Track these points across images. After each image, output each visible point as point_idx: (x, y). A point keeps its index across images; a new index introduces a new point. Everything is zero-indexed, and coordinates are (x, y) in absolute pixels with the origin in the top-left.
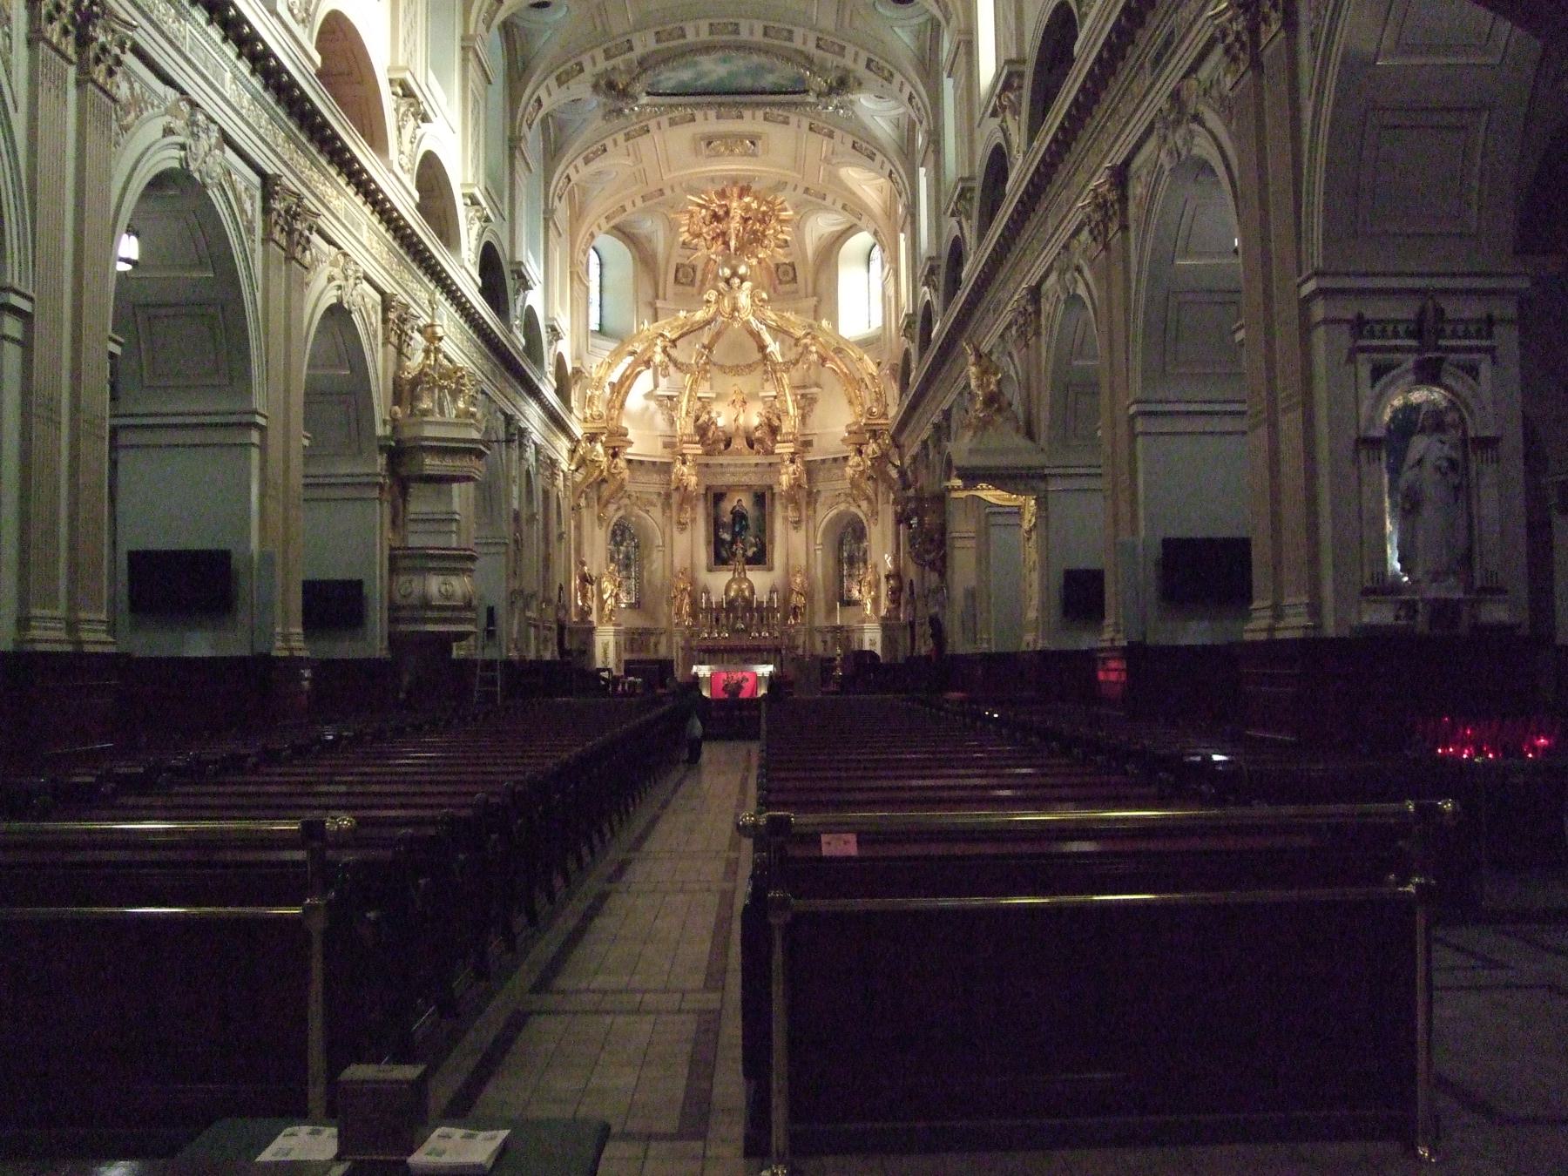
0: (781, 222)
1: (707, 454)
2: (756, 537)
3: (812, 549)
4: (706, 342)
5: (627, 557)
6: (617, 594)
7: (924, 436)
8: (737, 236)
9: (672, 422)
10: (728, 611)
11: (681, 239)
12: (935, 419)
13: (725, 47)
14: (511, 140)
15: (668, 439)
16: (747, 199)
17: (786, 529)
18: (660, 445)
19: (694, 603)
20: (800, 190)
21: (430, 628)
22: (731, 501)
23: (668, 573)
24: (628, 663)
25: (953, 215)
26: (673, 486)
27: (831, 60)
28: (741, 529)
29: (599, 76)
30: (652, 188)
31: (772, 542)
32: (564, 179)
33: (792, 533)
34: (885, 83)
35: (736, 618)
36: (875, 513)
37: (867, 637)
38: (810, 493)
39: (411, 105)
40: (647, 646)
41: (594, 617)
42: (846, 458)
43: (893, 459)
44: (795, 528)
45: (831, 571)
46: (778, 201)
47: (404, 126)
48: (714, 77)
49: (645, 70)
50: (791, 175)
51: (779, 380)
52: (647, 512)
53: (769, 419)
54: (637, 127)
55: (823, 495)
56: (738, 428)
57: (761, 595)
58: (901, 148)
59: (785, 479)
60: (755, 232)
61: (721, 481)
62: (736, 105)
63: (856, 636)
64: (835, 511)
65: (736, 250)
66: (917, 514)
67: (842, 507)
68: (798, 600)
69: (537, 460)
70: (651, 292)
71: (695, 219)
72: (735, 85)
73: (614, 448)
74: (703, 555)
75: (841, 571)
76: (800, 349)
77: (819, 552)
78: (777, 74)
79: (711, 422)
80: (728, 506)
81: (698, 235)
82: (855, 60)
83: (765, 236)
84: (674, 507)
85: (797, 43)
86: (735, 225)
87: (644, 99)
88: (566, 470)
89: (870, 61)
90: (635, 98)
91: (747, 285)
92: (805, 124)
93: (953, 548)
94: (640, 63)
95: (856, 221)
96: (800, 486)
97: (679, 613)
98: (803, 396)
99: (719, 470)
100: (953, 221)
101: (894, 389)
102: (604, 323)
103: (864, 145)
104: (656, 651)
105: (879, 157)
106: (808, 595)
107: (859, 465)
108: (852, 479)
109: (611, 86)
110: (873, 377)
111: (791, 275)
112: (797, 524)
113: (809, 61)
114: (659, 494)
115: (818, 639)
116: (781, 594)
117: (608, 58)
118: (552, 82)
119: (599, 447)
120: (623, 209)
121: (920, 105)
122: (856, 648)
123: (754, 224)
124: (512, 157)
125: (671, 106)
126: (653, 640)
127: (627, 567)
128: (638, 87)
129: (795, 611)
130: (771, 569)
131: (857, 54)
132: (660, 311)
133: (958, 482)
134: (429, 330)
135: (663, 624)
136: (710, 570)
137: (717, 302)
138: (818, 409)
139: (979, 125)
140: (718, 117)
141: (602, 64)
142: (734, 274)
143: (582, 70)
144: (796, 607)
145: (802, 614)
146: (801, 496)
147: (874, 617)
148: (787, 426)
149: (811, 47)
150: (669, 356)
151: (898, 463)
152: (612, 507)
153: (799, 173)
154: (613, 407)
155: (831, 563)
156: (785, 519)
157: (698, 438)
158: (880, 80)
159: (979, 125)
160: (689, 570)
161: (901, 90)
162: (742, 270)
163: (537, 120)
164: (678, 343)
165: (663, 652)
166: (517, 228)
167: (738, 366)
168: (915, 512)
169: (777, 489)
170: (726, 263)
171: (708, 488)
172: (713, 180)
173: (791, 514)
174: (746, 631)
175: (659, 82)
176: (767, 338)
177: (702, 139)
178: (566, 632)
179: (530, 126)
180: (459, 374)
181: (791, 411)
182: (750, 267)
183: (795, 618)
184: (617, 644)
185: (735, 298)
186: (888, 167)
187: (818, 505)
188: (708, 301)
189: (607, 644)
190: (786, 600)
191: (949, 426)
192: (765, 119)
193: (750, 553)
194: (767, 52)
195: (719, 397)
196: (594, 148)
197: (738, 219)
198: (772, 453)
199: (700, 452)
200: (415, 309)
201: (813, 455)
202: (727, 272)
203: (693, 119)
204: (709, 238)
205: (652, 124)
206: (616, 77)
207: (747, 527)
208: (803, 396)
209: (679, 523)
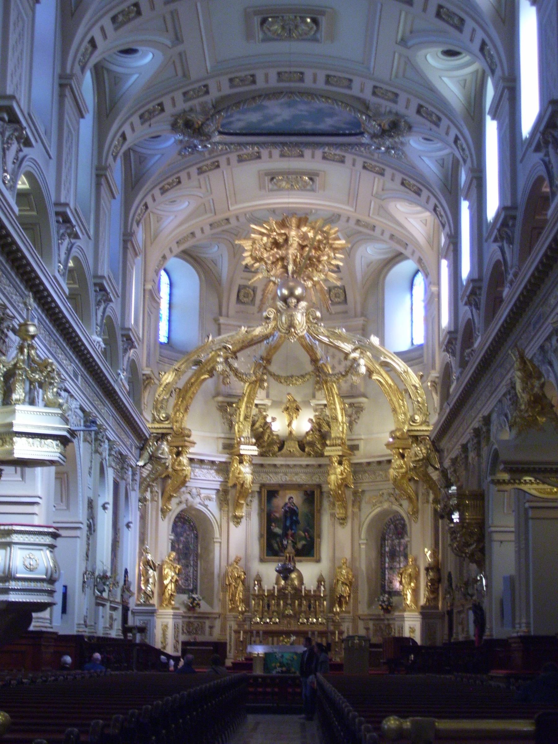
0: (335, 250)
1: (261, 455)
2: (304, 532)
3: (356, 547)
4: (264, 355)
5: (186, 547)
6: (177, 581)
7: (464, 441)
8: (295, 261)
9: (231, 426)
10: (279, 598)
11: (244, 263)
12: (476, 424)
13: (291, 93)
14: (97, 169)
15: (227, 442)
16: (304, 229)
17: (334, 525)
18: (221, 447)
19: (247, 589)
20: (352, 222)
21: (13, 597)
23: (224, 564)
24: (184, 644)
25: (495, 241)
26: (230, 484)
27: (386, 105)
28: (292, 524)
29: (176, 117)
30: (221, 216)
31: (319, 536)
32: (142, 207)
33: (339, 529)
34: (434, 127)
35: (286, 604)
36: (415, 512)
37: (407, 625)
38: (355, 493)
39: (16, 130)
40: (203, 628)
41: (155, 601)
42: (389, 462)
43: (433, 462)
44: (341, 524)
45: (373, 565)
46: (333, 231)
47: (8, 148)
48: (279, 120)
49: (219, 112)
50: (346, 209)
51: (330, 391)
52: (206, 506)
53: (319, 425)
54: (209, 162)
56: (291, 433)
57: (310, 583)
58: (445, 186)
59: (333, 477)
60: (310, 259)
61: (274, 479)
62: (297, 145)
63: (397, 623)
64: (378, 510)
65: (294, 272)
66: (459, 511)
67: (386, 506)
68: (345, 590)
69: (110, 455)
70: (216, 309)
71: (257, 246)
72: (297, 128)
73: (177, 447)
74: (255, 549)
75: (383, 562)
76: (348, 363)
77: (363, 547)
78: (336, 118)
79: (266, 426)
80: (280, 502)
81: (261, 260)
82: (407, 107)
83: (319, 261)
84: (230, 502)
85: (355, 91)
86: (292, 251)
87: (217, 138)
88: (134, 466)
89: (420, 107)
90: (209, 137)
91: (303, 304)
92: (360, 162)
93: (491, 541)
94: (214, 107)
95: (402, 250)
96: (347, 486)
97: (232, 600)
98: (351, 405)
99: (272, 469)
100: (495, 247)
101: (436, 398)
102: (173, 336)
103: (412, 182)
104: (211, 634)
105: (425, 193)
106: (350, 584)
107: (401, 467)
108: (395, 480)
109: (188, 124)
110: (416, 388)
111: (342, 298)
112: (343, 521)
113: (365, 106)
115: (361, 625)
116: (327, 586)
117: (185, 101)
118: (135, 119)
119: (165, 447)
120: (193, 234)
121: (465, 146)
122: (397, 635)
123: (310, 251)
124: (98, 185)
125: (240, 144)
126: (208, 623)
128: (211, 127)
129: (340, 600)
130: (318, 561)
131: (408, 101)
132: (222, 327)
133: (506, 476)
134: (23, 328)
135: (217, 609)
136: (262, 560)
137: (275, 319)
138: (364, 417)
139: (521, 161)
140: (282, 155)
141: (181, 105)
142: (292, 294)
143: (163, 110)
144: (341, 596)
145: (347, 603)
146: (349, 494)
147: (414, 607)
149: (367, 95)
150: (230, 366)
151: (438, 466)
152: (174, 501)
153: (352, 207)
154: (178, 410)
155: (374, 554)
156: (333, 515)
157: (254, 440)
158: (429, 124)
159: (521, 161)
160: (242, 563)
161: (447, 134)
162: (298, 291)
163: (121, 154)
164: (238, 354)
165: (216, 636)
166: (101, 246)
167: (292, 376)
168: (458, 508)
169: (325, 489)
170: (284, 285)
171: (262, 486)
172: (274, 211)
173: (339, 512)
174: (296, 616)
175: (230, 123)
176: (320, 352)
177: (267, 174)
178: (130, 613)
179: (115, 158)
180: (49, 369)
181: (340, 418)
182: (305, 288)
183: (340, 606)
184: (176, 627)
185: (292, 316)
186: (433, 201)
188: (267, 318)
189: (166, 626)
190: (333, 589)
191: (489, 431)
192: (324, 158)
193: (300, 545)
194: (327, 98)
195: (276, 404)
196: (170, 180)
197: (295, 245)
198: (322, 455)
199: (256, 453)
200: (11, 311)
201: (360, 457)
202: (285, 292)
203: (259, 157)
204: (269, 262)
205: (223, 160)
206: (192, 116)
207: (297, 522)
208: (351, 405)
209: (236, 517)
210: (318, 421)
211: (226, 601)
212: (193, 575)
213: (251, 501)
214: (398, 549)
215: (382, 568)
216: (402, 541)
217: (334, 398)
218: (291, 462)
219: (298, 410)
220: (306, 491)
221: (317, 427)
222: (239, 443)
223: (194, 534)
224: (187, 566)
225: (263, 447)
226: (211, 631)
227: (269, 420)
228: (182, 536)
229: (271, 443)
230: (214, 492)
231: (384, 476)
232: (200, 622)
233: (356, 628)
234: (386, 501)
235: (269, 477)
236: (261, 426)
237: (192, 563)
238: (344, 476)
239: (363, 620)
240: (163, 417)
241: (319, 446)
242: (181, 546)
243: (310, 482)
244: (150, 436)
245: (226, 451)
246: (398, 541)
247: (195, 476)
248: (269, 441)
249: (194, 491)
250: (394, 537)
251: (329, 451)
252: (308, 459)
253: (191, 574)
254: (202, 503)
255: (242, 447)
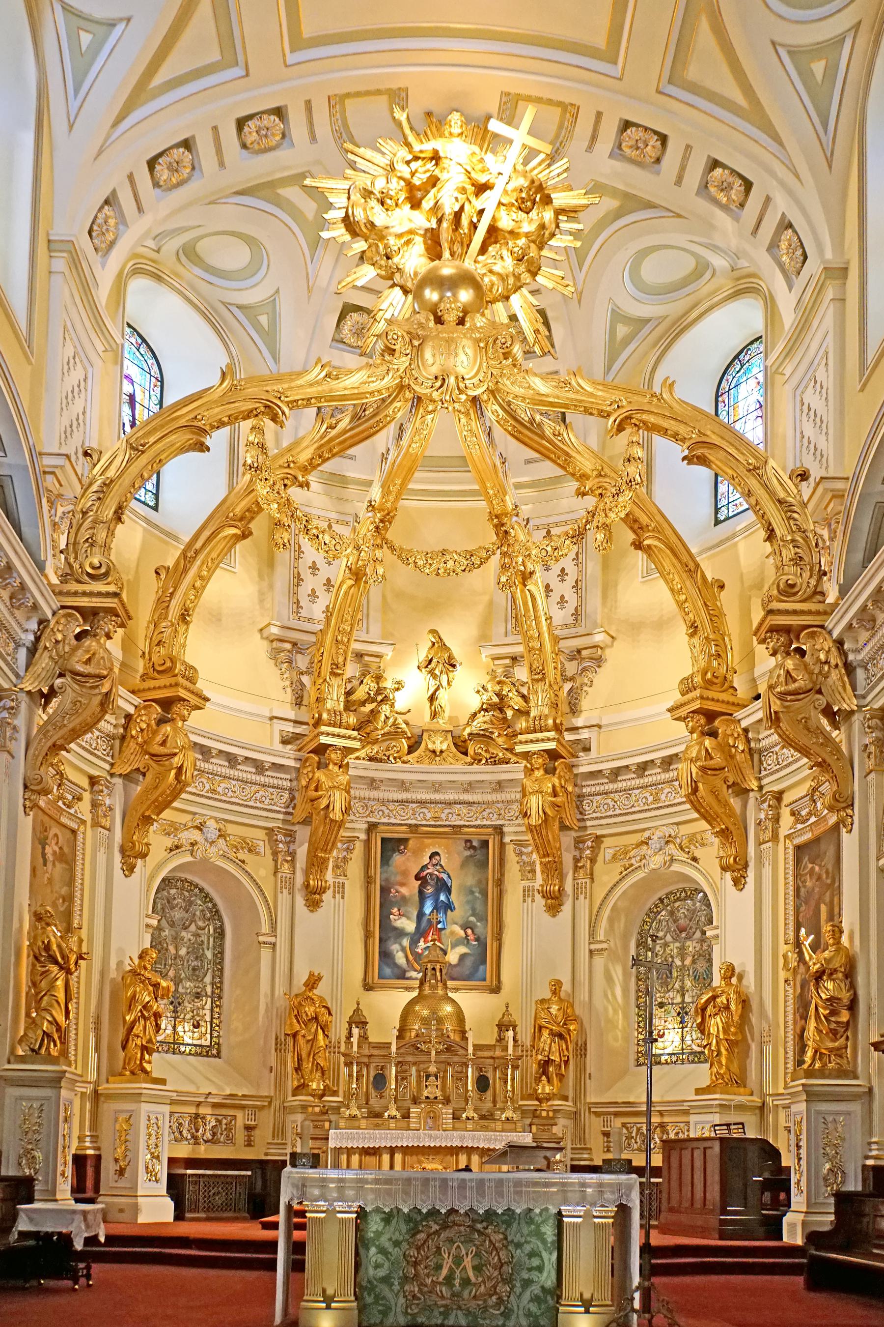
5: (196, 951)
22: (418, 852)
55: (607, 842)
64: (640, 875)
79: (381, 697)
114: (270, 831)
127: (196, 974)
148: (540, 706)
157: (352, 720)
171: (372, 827)
187: (600, 858)
199: (357, 744)
210: (497, 688)
211: (286, 1076)
212: (212, 1018)
213: (345, 859)
214: (678, 962)
215: (638, 1006)
216: (692, 946)
217: (538, 624)
218: (436, 772)
219: (454, 666)
220: (469, 841)
221: (495, 699)
222: (318, 723)
223: (215, 929)
224: (198, 996)
225: (376, 741)
226: (249, 1136)
227: (388, 684)
228: (186, 928)
229: (395, 733)
230: (261, 834)
231: (651, 799)
232: (225, 1116)
233: (580, 1135)
234: (655, 854)
235: (387, 811)
236: (370, 699)
237: (209, 989)
238: (558, 800)
239: (597, 1114)
240: (93, 568)
241: (500, 741)
242: (183, 952)
243: (478, 823)
244: (54, 614)
245: (289, 747)
246: (677, 944)
247: (214, 791)
248: (386, 729)
249: (211, 824)
250: (669, 938)
251: (526, 742)
252: (475, 766)
253: (208, 1013)
254: (232, 855)
255: (324, 728)
